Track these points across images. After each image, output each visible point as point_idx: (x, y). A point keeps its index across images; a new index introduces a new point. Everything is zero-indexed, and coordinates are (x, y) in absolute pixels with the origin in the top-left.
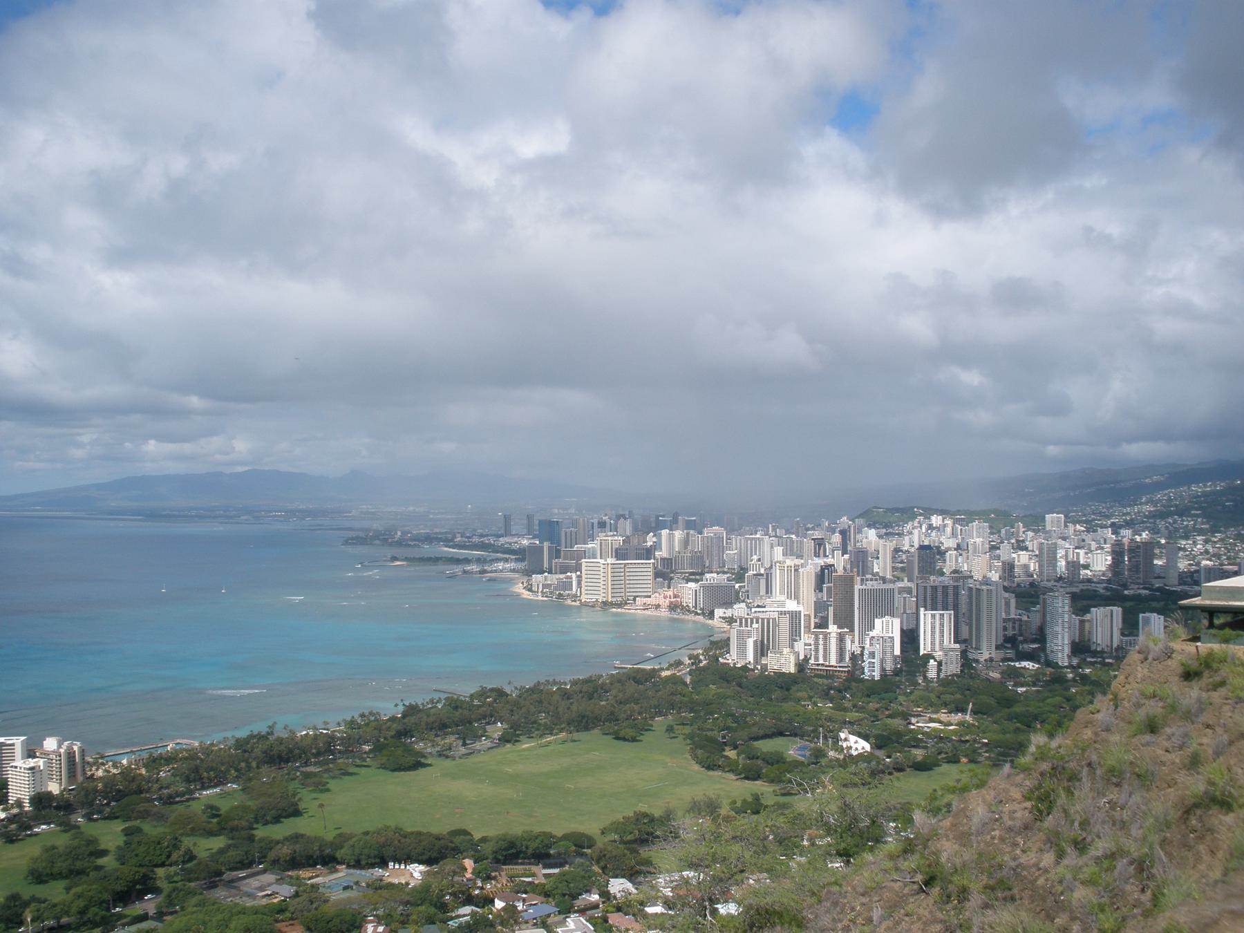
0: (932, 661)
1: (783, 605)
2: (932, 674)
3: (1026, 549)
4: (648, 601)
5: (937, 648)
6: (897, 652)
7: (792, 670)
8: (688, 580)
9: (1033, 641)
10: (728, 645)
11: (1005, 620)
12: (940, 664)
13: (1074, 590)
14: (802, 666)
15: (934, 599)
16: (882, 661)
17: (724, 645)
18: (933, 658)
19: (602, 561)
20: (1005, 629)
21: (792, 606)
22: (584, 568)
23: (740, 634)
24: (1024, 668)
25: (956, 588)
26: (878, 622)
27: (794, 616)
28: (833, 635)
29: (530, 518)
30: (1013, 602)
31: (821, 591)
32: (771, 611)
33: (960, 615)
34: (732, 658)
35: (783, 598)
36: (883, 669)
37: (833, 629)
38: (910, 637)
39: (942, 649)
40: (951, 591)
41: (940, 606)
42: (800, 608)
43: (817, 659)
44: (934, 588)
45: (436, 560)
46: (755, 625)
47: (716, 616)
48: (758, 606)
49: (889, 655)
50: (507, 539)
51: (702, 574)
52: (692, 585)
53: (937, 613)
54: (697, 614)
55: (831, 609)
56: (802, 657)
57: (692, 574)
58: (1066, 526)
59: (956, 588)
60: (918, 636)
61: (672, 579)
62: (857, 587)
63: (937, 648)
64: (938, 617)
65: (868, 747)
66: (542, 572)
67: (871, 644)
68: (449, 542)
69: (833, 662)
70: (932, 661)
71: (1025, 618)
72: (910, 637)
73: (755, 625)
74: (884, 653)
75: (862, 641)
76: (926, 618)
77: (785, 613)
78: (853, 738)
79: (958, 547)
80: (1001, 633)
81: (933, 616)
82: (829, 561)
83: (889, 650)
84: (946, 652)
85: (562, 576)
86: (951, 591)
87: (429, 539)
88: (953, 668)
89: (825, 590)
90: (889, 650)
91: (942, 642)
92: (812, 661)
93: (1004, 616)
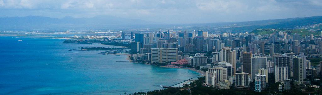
0: (280, 85)
1: (225, 64)
2: (280, 90)
3: (314, 44)
4: (175, 63)
5: (282, 80)
6: (267, 81)
7: (228, 88)
8: (190, 56)
9: (318, 78)
10: (205, 79)
11: (307, 70)
12: (283, 86)
14: (232, 87)
15: (280, 62)
16: (262, 84)
17: (202, 79)
19: (158, 49)
20: (307, 73)
21: (228, 65)
22: (152, 51)
23: (209, 75)
24: (314, 88)
25: (288, 58)
26: (260, 70)
27: (229, 68)
28: (243, 75)
29: (132, 33)
30: (310, 63)
31: (238, 59)
32: (220, 67)
33: (290, 68)
34: (206, 84)
35: (224, 62)
36: (262, 88)
37: (243, 73)
38: (272, 76)
40: (286, 59)
41: (282, 65)
42: (231, 66)
43: (237, 84)
44: (280, 58)
45: (97, 49)
46: (214, 72)
47: (200, 69)
48: (216, 65)
49: (264, 83)
50: (124, 41)
51: (195, 53)
52: (191, 57)
53: (282, 67)
54: (193, 68)
55: (242, 66)
56: (232, 83)
57: (192, 53)
59: (288, 58)
60: (275, 76)
61: (184, 55)
62: (252, 58)
63: (282, 80)
64: (282, 69)
66: (137, 53)
67: (257, 79)
68: (103, 43)
69: (243, 85)
70: (280, 85)
71: (314, 69)
73: (214, 72)
74: (262, 82)
75: (254, 77)
76: (277, 69)
77: (225, 67)
79: (289, 43)
80: (305, 75)
81: (280, 69)
82: (241, 48)
83: (264, 81)
84: (285, 81)
85: (144, 54)
86: (286, 59)
87: (95, 41)
88: (288, 88)
89: (240, 59)
90: (264, 81)
91: (283, 78)
92: (236, 85)
93: (306, 68)
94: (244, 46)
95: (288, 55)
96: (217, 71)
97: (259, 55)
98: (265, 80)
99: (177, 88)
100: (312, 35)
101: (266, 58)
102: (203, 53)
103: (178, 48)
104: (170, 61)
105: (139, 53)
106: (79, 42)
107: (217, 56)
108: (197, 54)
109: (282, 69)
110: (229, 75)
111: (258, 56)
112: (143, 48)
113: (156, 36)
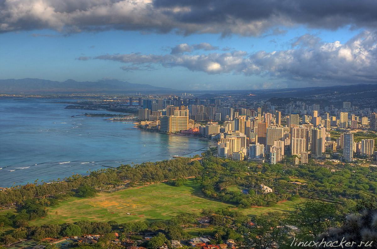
0: (296, 158)
6: (283, 154)
13: (354, 132)
18: (296, 156)
38: (288, 149)
39: (301, 153)
41: (300, 137)
58: (351, 107)
64: (299, 141)
65: (271, 191)
66: (144, 120)
72: (288, 149)
78: (265, 187)
83: (279, 153)
88: (304, 161)
94: (259, 115)
95: (306, 126)
96: (230, 142)
97: (275, 126)
98: (281, 152)
99: (188, 159)
100: (333, 106)
101: (283, 129)
102: (215, 121)
103: (189, 116)
104: (181, 129)
105: (148, 120)
106: (82, 108)
107: (230, 125)
108: (209, 123)
109: (299, 141)
110: (243, 145)
111: (274, 127)
112: (152, 116)
113: (165, 102)
